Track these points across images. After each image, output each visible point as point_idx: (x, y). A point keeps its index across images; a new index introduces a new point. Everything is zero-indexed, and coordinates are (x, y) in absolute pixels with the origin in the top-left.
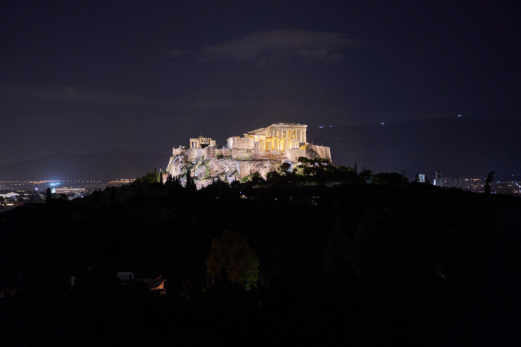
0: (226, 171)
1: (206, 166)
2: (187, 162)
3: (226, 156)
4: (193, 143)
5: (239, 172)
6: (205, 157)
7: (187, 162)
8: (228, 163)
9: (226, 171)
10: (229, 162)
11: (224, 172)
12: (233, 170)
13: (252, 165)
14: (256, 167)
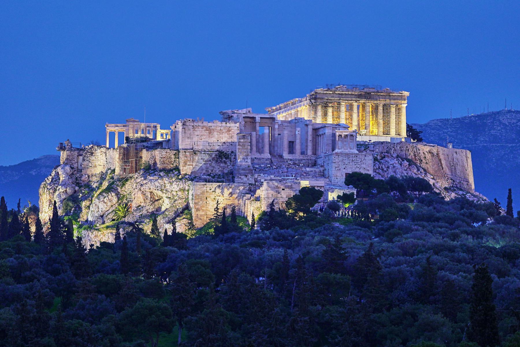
0: (163, 209)
1: (118, 194)
2: (78, 183)
3: (163, 170)
4: (112, 134)
5: (193, 211)
6: (117, 171)
7: (78, 184)
8: (168, 186)
9: (163, 209)
10: (171, 183)
11: (159, 209)
12: (180, 205)
13: (227, 192)
14: (239, 198)
